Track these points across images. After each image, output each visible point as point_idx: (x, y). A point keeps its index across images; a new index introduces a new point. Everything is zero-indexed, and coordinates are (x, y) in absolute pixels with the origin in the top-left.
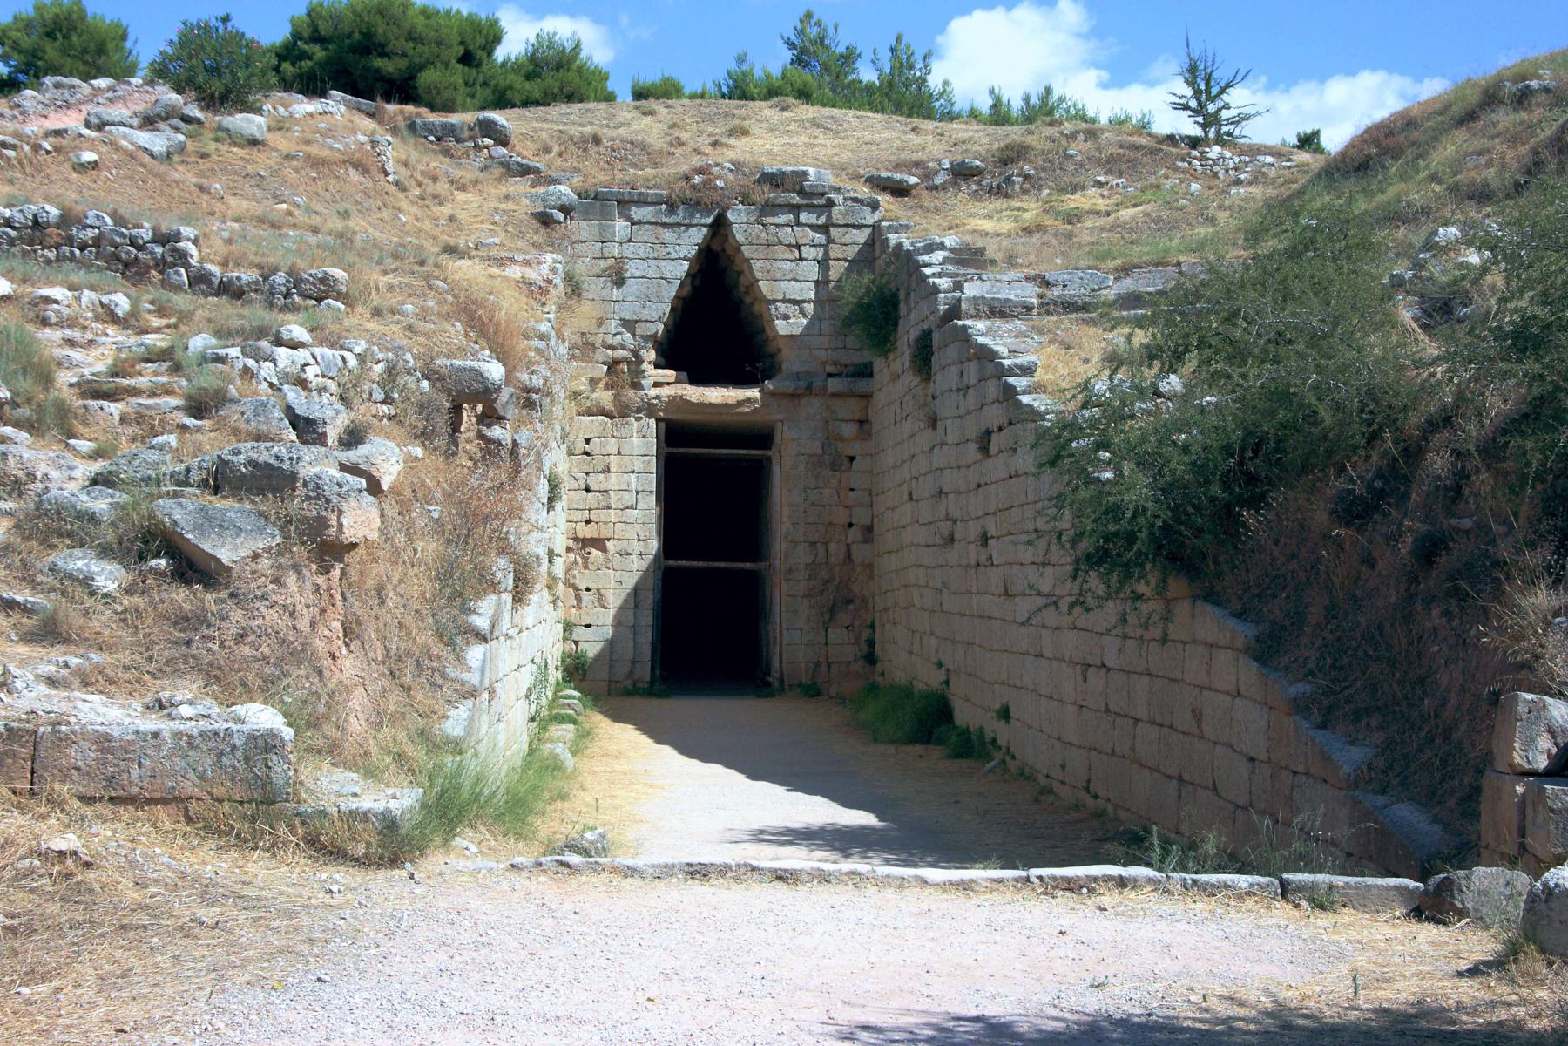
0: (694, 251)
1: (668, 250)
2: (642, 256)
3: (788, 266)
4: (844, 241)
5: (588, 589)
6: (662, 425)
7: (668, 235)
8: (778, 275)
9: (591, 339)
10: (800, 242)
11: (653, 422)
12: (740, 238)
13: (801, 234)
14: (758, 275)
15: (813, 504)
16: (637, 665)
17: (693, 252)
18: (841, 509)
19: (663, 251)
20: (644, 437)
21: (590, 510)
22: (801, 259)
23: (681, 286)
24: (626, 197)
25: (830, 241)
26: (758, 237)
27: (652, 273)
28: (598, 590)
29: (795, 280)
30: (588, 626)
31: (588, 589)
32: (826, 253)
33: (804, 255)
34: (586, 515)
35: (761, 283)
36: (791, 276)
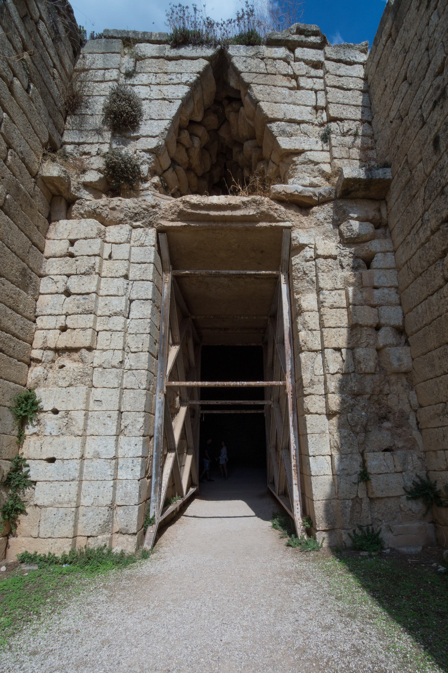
0: (193, 78)
1: (170, 77)
2: (146, 83)
3: (286, 92)
4: (338, 73)
5: (55, 412)
6: (163, 237)
7: (171, 66)
8: (278, 99)
9: (87, 148)
10: (297, 73)
11: (152, 232)
12: (239, 65)
13: (298, 67)
14: (259, 96)
15: (332, 307)
16: (120, 511)
17: (194, 78)
18: (367, 308)
19: (166, 78)
20: (142, 245)
21: (67, 315)
22: (299, 88)
23: (182, 106)
24: (131, 35)
25: (327, 72)
26: (258, 66)
27: (154, 95)
28: (67, 412)
29: (295, 104)
30: (52, 460)
31: (55, 412)
32: (325, 82)
33: (302, 84)
34: (61, 321)
35: (261, 104)
36: (290, 100)
